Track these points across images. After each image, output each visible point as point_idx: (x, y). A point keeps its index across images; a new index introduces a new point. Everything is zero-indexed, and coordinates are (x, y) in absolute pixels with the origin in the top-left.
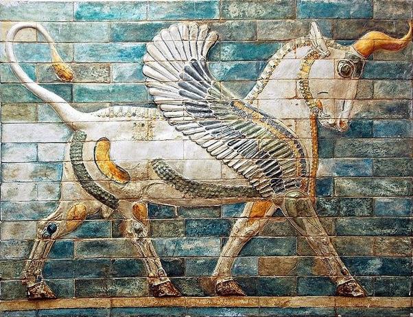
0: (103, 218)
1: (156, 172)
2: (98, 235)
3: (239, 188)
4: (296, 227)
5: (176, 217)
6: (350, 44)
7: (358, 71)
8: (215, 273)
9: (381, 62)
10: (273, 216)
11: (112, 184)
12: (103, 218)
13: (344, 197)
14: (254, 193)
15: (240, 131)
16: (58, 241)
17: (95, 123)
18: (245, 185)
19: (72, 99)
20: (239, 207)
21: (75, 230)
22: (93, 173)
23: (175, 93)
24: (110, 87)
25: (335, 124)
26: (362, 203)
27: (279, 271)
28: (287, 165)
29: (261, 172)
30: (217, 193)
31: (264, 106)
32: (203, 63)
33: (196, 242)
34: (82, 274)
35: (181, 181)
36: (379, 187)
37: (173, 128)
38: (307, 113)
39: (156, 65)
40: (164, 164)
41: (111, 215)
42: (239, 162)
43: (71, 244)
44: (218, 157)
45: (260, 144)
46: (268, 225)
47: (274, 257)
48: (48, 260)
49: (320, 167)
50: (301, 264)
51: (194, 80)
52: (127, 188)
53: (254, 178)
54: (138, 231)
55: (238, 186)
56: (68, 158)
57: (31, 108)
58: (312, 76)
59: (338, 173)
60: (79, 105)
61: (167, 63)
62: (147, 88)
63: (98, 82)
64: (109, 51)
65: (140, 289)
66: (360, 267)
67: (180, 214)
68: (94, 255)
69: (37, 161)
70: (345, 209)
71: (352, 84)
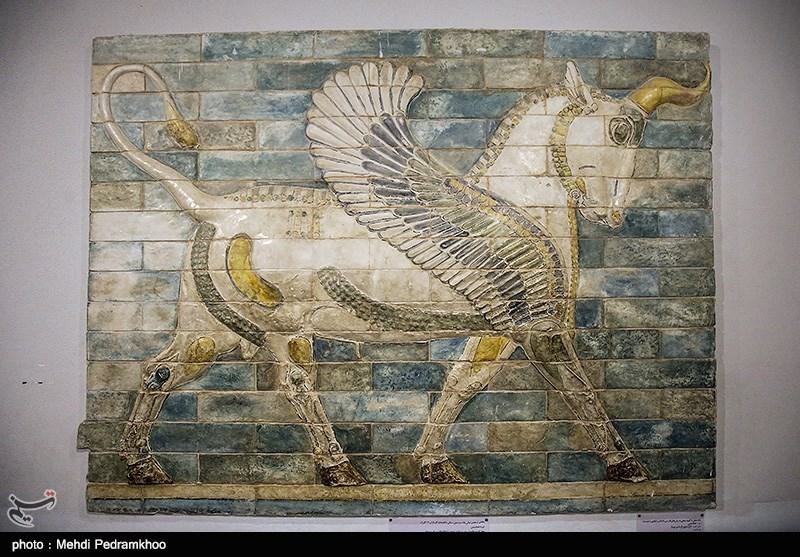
0: (243, 359)
1: (326, 289)
2: (234, 385)
7: (638, 136)
8: (420, 447)
9: (668, 123)
11: (255, 308)
12: (243, 359)
13: (617, 330)
14: (481, 323)
16: (173, 394)
17: (231, 217)
18: (469, 311)
19: (197, 174)
20: (457, 343)
21: (198, 377)
22: (224, 288)
23: (356, 165)
24: (255, 156)
25: (605, 216)
27: (520, 444)
28: (534, 279)
29: (493, 290)
30: (423, 324)
31: (498, 187)
32: (401, 121)
33: (390, 400)
34: (210, 447)
35: (365, 304)
36: (667, 312)
37: (352, 219)
40: (339, 276)
42: (459, 274)
43: (193, 399)
46: (503, 372)
49: (582, 281)
50: (553, 434)
51: (387, 145)
54: (297, 382)
56: (188, 266)
57: (134, 189)
58: (570, 141)
59: (608, 292)
60: (205, 184)
61: (345, 120)
62: (312, 158)
63: (236, 150)
64: (255, 103)
65: (301, 472)
68: (230, 418)
71: (627, 155)
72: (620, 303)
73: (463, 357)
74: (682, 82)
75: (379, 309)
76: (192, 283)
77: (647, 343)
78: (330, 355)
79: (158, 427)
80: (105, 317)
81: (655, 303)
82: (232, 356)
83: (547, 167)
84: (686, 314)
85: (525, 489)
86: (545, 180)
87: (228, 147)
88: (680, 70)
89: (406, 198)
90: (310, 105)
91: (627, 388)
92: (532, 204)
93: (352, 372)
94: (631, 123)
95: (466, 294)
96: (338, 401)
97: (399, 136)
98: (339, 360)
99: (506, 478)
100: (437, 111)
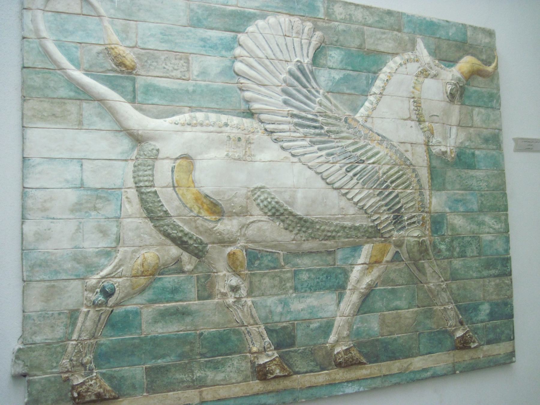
1: (258, 205)
2: (177, 297)
3: (359, 226)
4: (416, 273)
5: (282, 267)
6: (452, 66)
7: (461, 96)
8: (332, 338)
10: (392, 261)
12: (183, 272)
15: (359, 153)
19: (134, 98)
21: (143, 290)
24: (189, 86)
25: (446, 152)
26: (471, 242)
30: (334, 234)
33: (309, 300)
34: (156, 358)
35: (291, 218)
36: (483, 223)
37: (276, 146)
38: (421, 138)
39: (252, 61)
40: (269, 194)
41: (196, 267)
43: (137, 314)
44: (336, 185)
45: (381, 172)
47: (395, 312)
48: (103, 340)
49: (434, 201)
52: (220, 227)
53: (376, 212)
54: (235, 289)
55: (357, 225)
56: (130, 182)
57: (72, 107)
59: (450, 208)
60: (144, 107)
61: (267, 62)
62: (239, 92)
65: (239, 371)
66: (473, 315)
67: (286, 263)
69: (82, 186)
70: (458, 249)
71: (456, 108)
72: (457, 217)
73: (360, 261)
74: (482, 61)
75: (302, 222)
76: (136, 200)
77: (474, 246)
78: (260, 264)
79: (102, 345)
80: (40, 237)
81: (476, 216)
82: (173, 269)
83: (410, 114)
84: (493, 224)
85: (405, 363)
86: (409, 122)
87: (165, 75)
88: (481, 52)
89: (317, 131)
90: (236, 45)
91: (463, 279)
92: (403, 141)
93: (278, 278)
94: (458, 86)
95: (365, 208)
96: (268, 304)
97: (309, 81)
98: (267, 269)
99: (393, 357)
100: (334, 63)
